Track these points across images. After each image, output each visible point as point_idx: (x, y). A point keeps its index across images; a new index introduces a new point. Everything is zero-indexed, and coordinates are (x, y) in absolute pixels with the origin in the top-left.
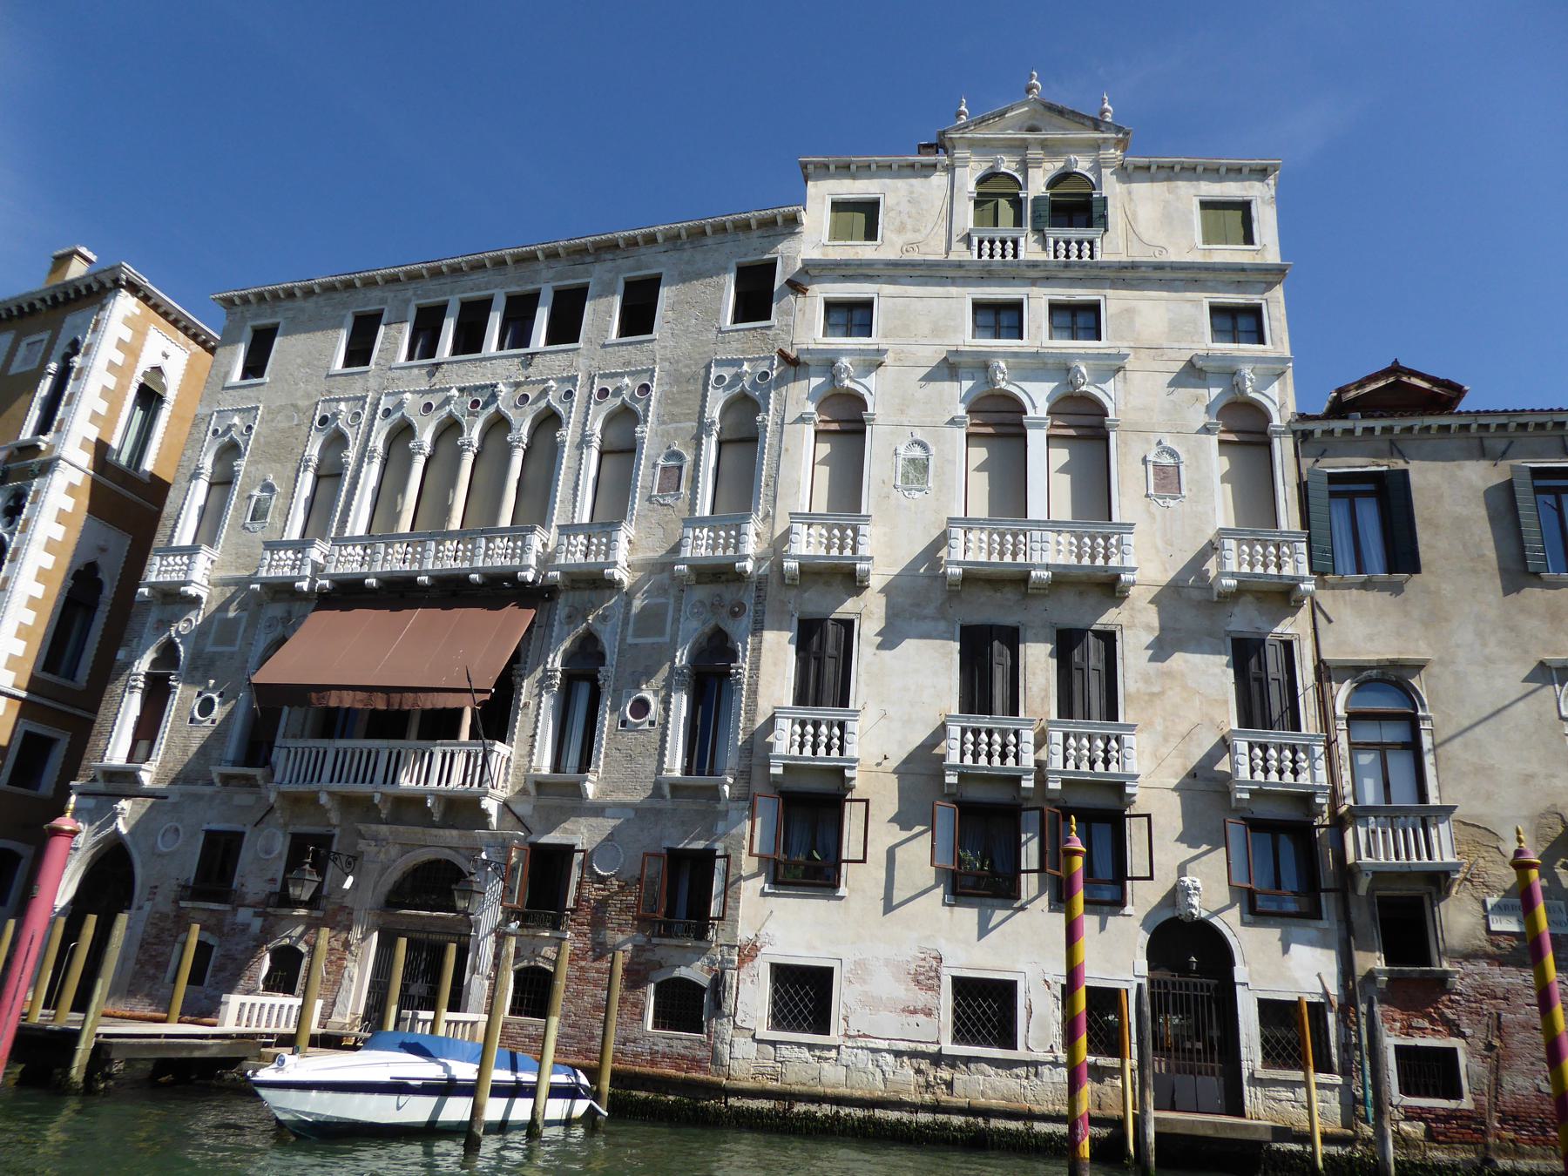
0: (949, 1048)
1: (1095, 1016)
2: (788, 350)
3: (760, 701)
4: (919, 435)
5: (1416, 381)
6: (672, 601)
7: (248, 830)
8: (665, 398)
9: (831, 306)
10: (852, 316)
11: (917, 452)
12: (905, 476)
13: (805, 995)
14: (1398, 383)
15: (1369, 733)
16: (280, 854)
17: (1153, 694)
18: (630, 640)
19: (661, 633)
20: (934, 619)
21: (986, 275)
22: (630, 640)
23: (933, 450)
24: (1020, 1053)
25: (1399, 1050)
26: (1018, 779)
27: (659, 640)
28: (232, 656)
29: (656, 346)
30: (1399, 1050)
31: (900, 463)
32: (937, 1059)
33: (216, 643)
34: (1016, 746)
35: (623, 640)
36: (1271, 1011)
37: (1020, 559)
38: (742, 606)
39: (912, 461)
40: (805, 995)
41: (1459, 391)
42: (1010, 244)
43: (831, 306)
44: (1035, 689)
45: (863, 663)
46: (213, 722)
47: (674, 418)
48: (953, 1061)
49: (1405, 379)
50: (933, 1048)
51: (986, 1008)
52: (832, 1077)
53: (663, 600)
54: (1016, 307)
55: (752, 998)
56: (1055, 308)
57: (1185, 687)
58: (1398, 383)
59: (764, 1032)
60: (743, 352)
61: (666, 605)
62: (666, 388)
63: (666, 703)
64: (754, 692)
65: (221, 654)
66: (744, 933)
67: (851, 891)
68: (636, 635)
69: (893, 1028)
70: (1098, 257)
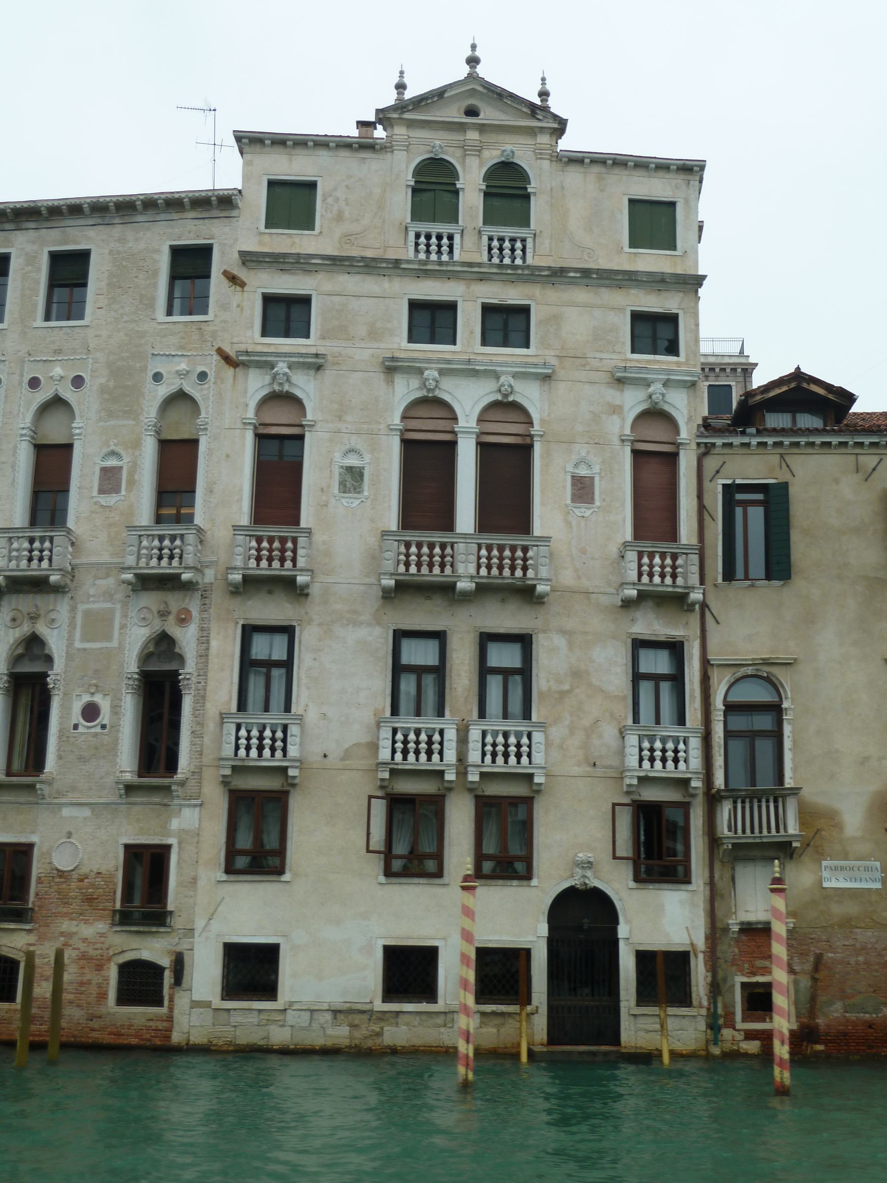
0: (379, 1005)
1: (500, 974)
2: (227, 349)
3: (208, 705)
4: (356, 442)
5: (814, 388)
6: (118, 606)
8: (103, 390)
9: (269, 300)
10: (286, 314)
13: (252, 969)
14: (798, 388)
15: (740, 722)
17: (563, 694)
18: (78, 645)
19: (108, 637)
20: (369, 625)
21: (423, 273)
22: (78, 645)
25: (744, 985)
26: (441, 773)
27: (108, 645)
29: (90, 333)
30: (744, 985)
31: (337, 472)
32: (370, 1013)
36: (644, 958)
38: (188, 612)
39: (350, 469)
40: (252, 969)
41: (850, 398)
42: (445, 241)
43: (269, 300)
47: (111, 414)
48: (383, 1016)
49: (805, 385)
51: (409, 971)
54: (451, 307)
55: (206, 974)
56: (488, 310)
58: (798, 388)
59: (217, 1002)
60: (182, 348)
61: (112, 611)
62: (103, 380)
63: (116, 709)
64: (201, 699)
69: (332, 993)
70: (530, 260)
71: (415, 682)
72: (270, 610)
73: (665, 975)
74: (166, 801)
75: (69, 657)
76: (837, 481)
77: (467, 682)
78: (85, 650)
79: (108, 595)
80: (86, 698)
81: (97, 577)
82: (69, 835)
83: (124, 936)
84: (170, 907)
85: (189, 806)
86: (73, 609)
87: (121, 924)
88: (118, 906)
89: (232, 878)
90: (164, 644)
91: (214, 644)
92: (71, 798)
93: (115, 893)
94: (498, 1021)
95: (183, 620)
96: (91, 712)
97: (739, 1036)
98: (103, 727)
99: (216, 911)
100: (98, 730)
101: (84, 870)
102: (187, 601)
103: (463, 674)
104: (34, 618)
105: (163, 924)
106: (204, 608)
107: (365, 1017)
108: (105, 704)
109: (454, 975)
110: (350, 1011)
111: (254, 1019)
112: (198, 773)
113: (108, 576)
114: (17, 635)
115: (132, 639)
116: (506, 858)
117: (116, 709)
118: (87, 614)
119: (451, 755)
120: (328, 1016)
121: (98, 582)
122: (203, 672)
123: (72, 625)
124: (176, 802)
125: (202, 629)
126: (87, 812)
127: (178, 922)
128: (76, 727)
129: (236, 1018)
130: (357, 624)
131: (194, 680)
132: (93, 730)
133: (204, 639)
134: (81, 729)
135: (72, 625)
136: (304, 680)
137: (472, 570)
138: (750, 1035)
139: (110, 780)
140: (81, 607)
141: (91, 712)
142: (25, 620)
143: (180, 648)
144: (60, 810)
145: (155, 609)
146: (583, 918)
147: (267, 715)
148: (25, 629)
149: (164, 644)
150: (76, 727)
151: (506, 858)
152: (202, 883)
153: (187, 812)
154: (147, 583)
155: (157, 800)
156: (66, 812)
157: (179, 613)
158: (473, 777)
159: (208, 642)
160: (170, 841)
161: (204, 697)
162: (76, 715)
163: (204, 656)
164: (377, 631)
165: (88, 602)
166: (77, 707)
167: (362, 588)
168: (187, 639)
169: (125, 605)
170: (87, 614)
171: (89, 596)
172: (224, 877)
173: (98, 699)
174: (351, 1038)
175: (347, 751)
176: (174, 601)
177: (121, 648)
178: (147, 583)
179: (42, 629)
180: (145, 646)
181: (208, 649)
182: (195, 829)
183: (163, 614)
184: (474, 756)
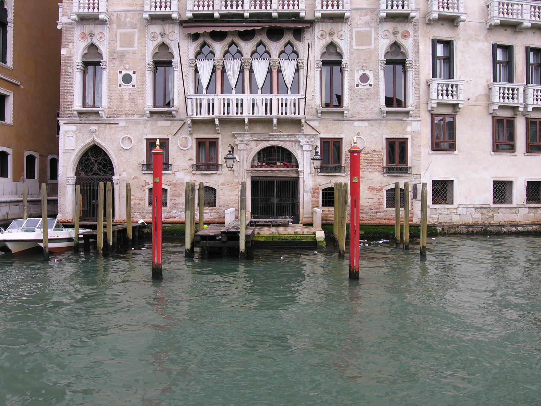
6: (373, 29)
7: (170, 137)
13: (442, 190)
16: (191, 148)
18: (355, 47)
19: (370, 44)
22: (355, 47)
24: (514, 205)
27: (370, 47)
28: (134, 53)
33: (121, 46)
34: (452, 91)
35: (351, 47)
37: (520, 17)
44: (519, 71)
45: (458, 59)
46: (134, 86)
50: (488, 206)
51: (502, 190)
52: (456, 219)
53: (368, 29)
61: (370, 32)
63: (376, 77)
64: (417, 73)
65: (128, 52)
67: (459, 151)
68: (357, 45)
72: (444, 33)
74: (405, 119)
75: (351, 53)
77: (521, 68)
78: (358, 50)
79: (368, 24)
80: (361, 72)
81: (360, 16)
82: (358, 134)
83: (389, 178)
84: (409, 165)
85: (415, 121)
86: (351, 30)
87: (387, 173)
88: (385, 165)
89: (435, 152)
90: (396, 46)
91: (421, 47)
92: (361, 117)
93: (382, 159)
94: (534, 211)
95: (405, 36)
96: (364, 78)
98: (371, 85)
99: (427, 166)
100: (368, 87)
101: (366, 150)
102: (406, 27)
103: (520, 64)
104: (331, 34)
105: (407, 173)
106: (416, 30)
107: (486, 210)
108: (371, 75)
109: (519, 193)
110: (481, 208)
111: (446, 212)
112: (418, 106)
113: (367, 15)
114: (324, 43)
115: (384, 45)
117: (376, 77)
118: (358, 33)
119: (521, 100)
120: (473, 210)
121: (361, 18)
122: (417, 60)
123: (351, 38)
124: (410, 119)
125: (415, 40)
126: (366, 124)
127: (414, 171)
128: (357, 85)
129: (439, 212)
130: (478, 41)
131: (413, 64)
132: (366, 87)
133: (416, 45)
134: (360, 86)
135: (351, 38)
136: (458, 66)
137: (529, 18)
139: (376, 110)
140: (354, 30)
141: (364, 78)
142: (327, 36)
143: (404, 49)
144: (353, 123)
145: (391, 31)
147: (451, 80)
148: (328, 40)
149: (396, 46)
150: (357, 85)
152: (422, 155)
153: (414, 124)
154: (392, 18)
155: (401, 118)
156: (356, 124)
157: (403, 33)
158: (530, 110)
159: (418, 46)
160: (407, 137)
161: (418, 72)
162: (357, 80)
163: (417, 53)
164: (486, 44)
165: (358, 27)
166: (357, 76)
167: (479, 24)
168: (408, 44)
169: (376, 29)
170: (358, 33)
171: (358, 24)
172: (432, 152)
173: (367, 72)
174: (482, 219)
175: (477, 97)
176: (401, 27)
177: (376, 49)
178: (392, 18)
179: (336, 40)
180: (387, 49)
181: (418, 50)
182: (418, 132)
183: (395, 33)
184: (530, 101)
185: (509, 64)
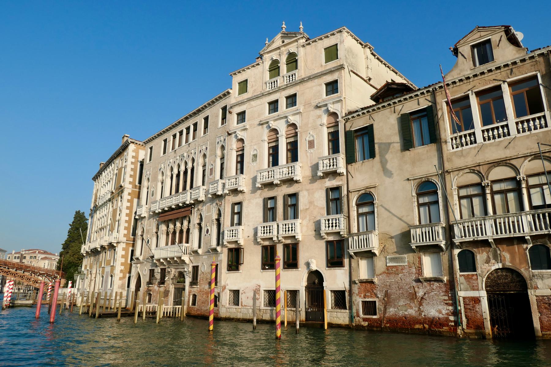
4: (255, 147)
11: (255, 153)
12: (252, 160)
17: (307, 209)
23: (258, 151)
31: (251, 156)
49: (390, 87)
51: (272, 298)
55: (226, 298)
57: (314, 205)
66: (223, 283)
71: (269, 213)
73: (340, 299)
76: (389, 118)
97: (361, 320)
116: (292, 263)
119: (275, 233)
138: (365, 320)
146: (316, 281)
151: (292, 263)
185: (273, 209)
